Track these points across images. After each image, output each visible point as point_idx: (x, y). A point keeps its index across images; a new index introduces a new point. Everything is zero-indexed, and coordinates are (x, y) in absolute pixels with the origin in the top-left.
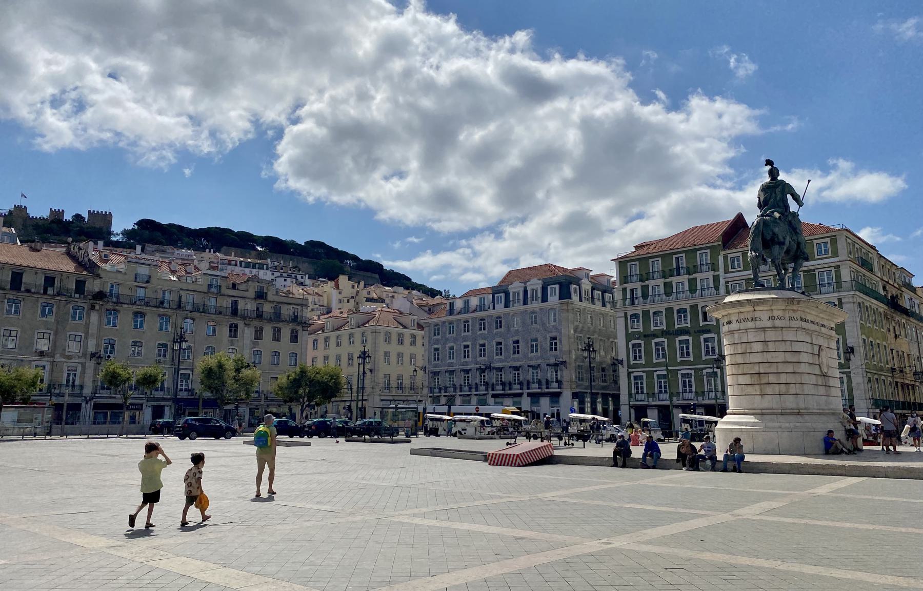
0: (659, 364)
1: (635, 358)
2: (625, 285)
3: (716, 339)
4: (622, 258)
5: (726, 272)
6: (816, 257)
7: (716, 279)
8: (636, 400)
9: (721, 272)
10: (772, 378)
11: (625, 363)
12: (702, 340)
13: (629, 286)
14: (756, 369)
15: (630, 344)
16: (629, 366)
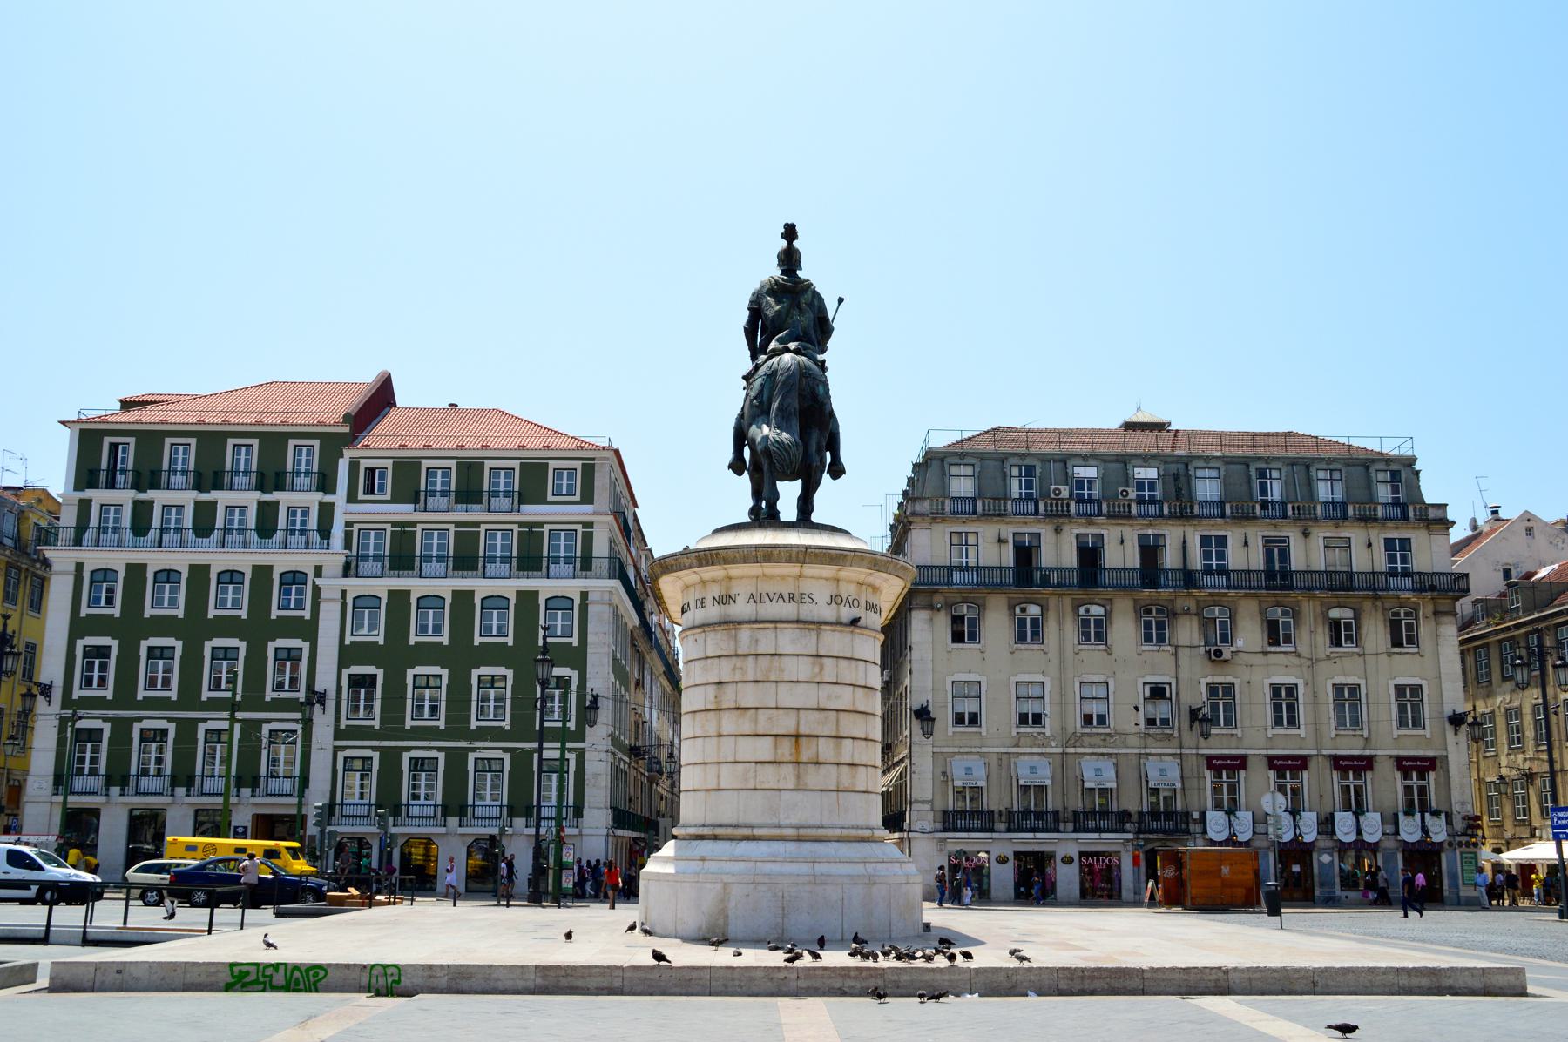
0: (214, 705)
1: (88, 682)
2: (89, 493)
3: (306, 654)
4: (87, 421)
5: (352, 498)
6: (550, 497)
7: (326, 511)
8: (138, 794)
9: (339, 498)
10: (825, 750)
11: (57, 694)
12: (143, 653)
13: (98, 496)
14: (786, 724)
15: (80, 644)
16: (67, 702)
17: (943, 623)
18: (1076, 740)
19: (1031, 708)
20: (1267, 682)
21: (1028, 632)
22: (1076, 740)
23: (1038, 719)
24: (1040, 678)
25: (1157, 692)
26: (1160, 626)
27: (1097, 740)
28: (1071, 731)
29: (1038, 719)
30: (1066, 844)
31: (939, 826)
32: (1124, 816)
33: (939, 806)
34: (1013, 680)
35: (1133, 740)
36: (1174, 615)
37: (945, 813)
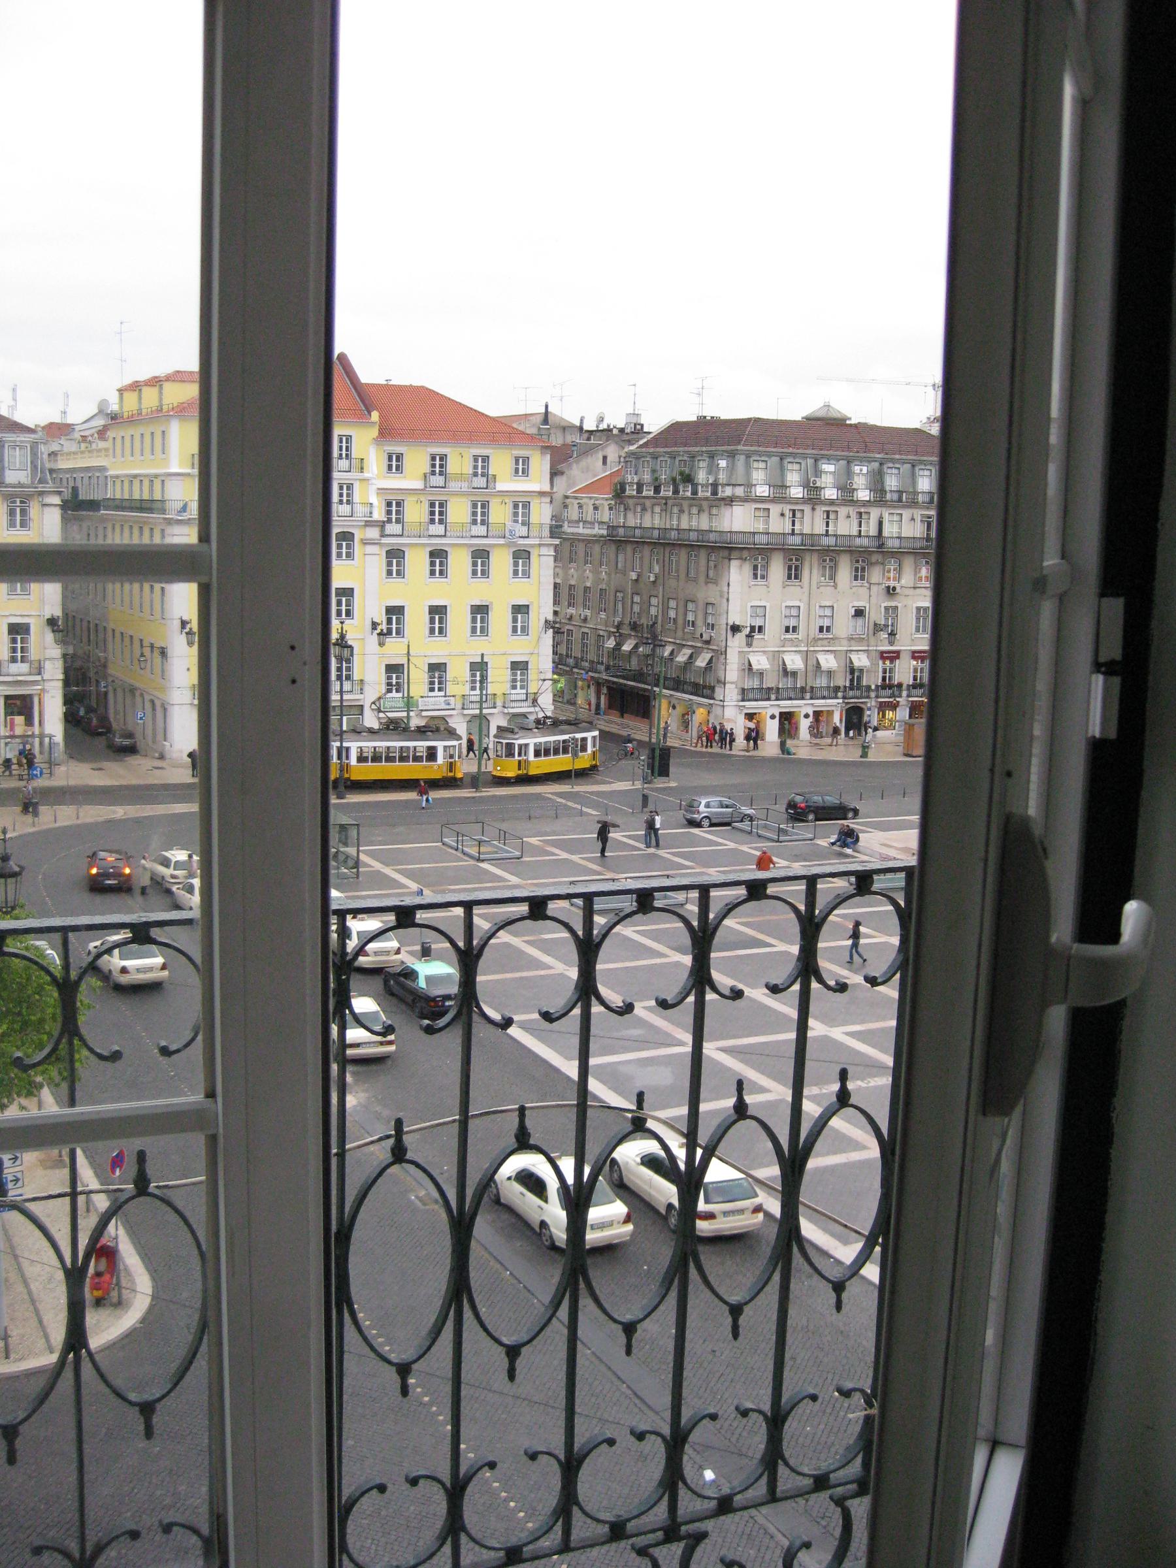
17: (747, 569)
18: (816, 640)
19: (792, 623)
20: (915, 605)
21: (793, 574)
22: (816, 640)
23: (795, 629)
24: (797, 603)
25: (859, 613)
26: (863, 569)
27: (825, 642)
28: (812, 636)
29: (795, 629)
30: (804, 708)
31: (740, 697)
32: (837, 689)
33: (740, 685)
34: (784, 605)
35: (845, 642)
36: (872, 564)
37: (743, 690)
